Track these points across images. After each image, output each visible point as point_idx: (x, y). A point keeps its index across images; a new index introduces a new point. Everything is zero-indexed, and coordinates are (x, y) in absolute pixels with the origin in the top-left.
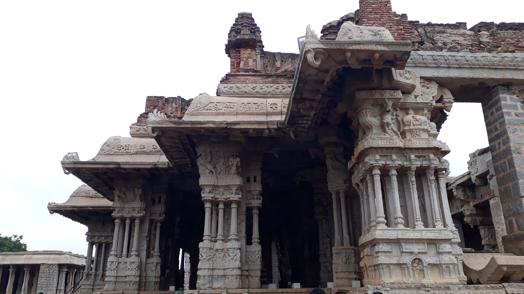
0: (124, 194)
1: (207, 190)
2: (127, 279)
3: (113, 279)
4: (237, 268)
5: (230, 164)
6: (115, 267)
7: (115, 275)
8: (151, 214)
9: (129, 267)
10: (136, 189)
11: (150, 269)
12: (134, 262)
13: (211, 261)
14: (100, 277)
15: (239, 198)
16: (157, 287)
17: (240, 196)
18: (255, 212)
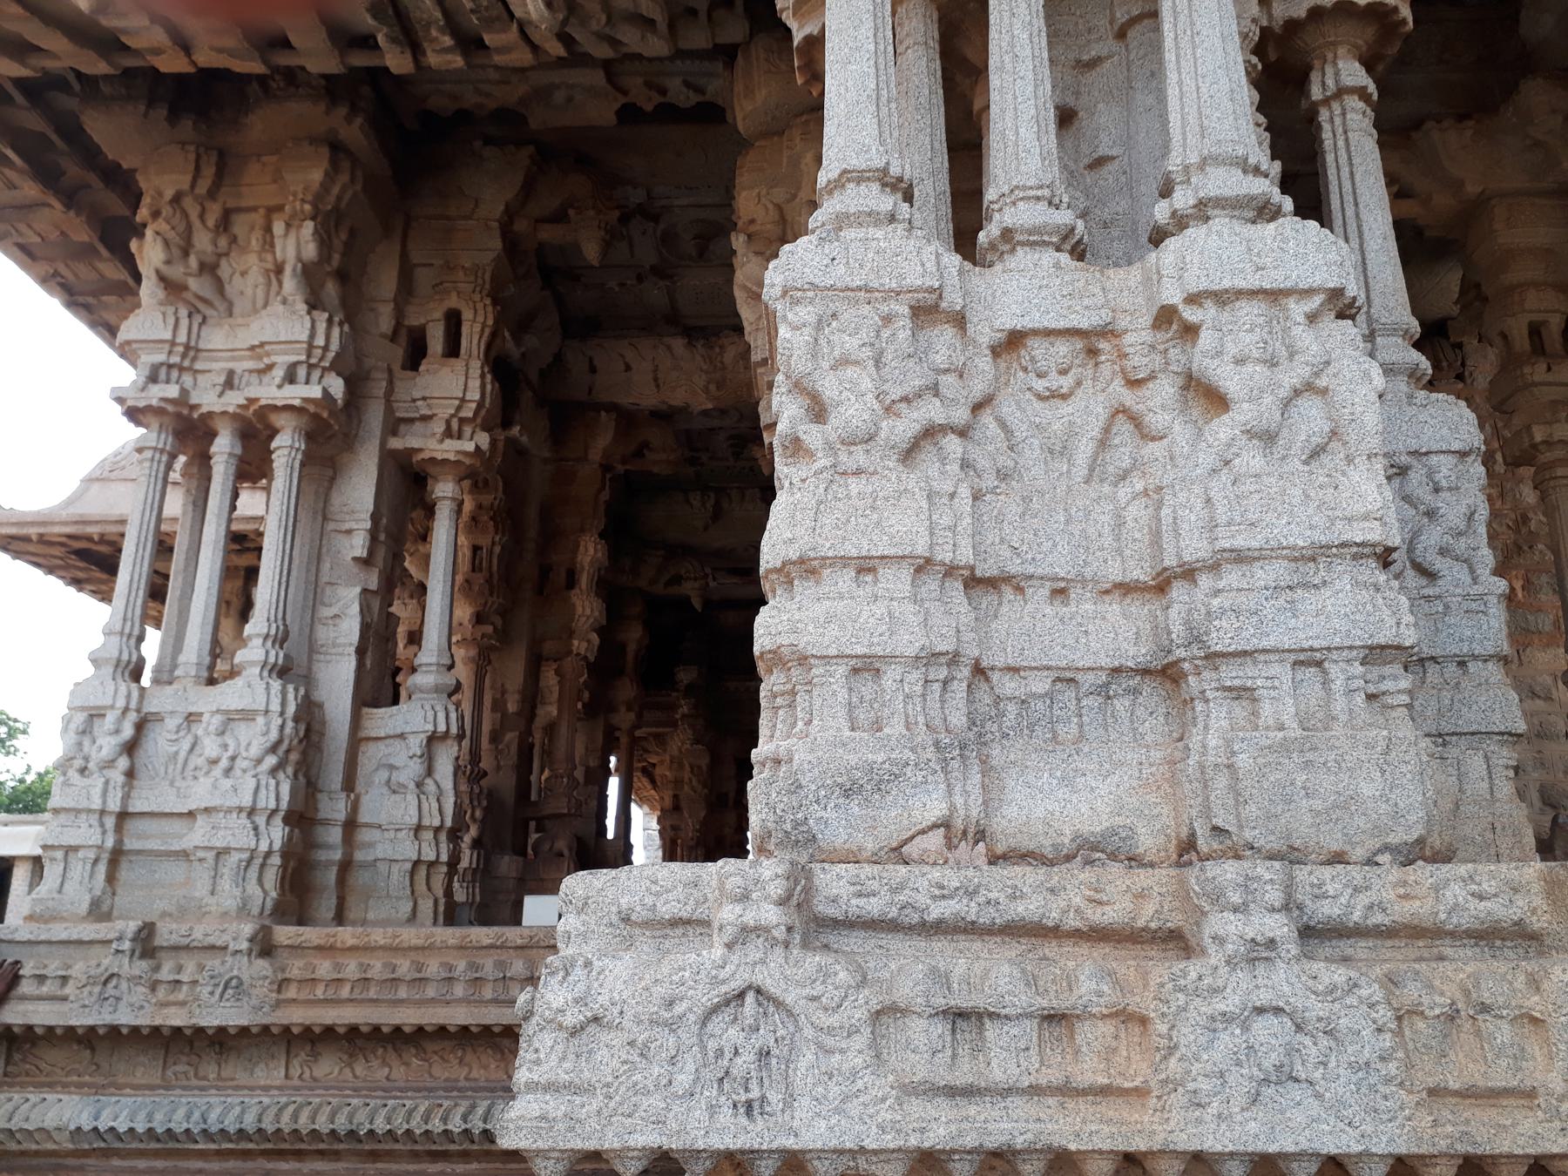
0: (209, 269)
8: (394, 425)
9: (210, 747)
11: (384, 774)
12: (247, 715)
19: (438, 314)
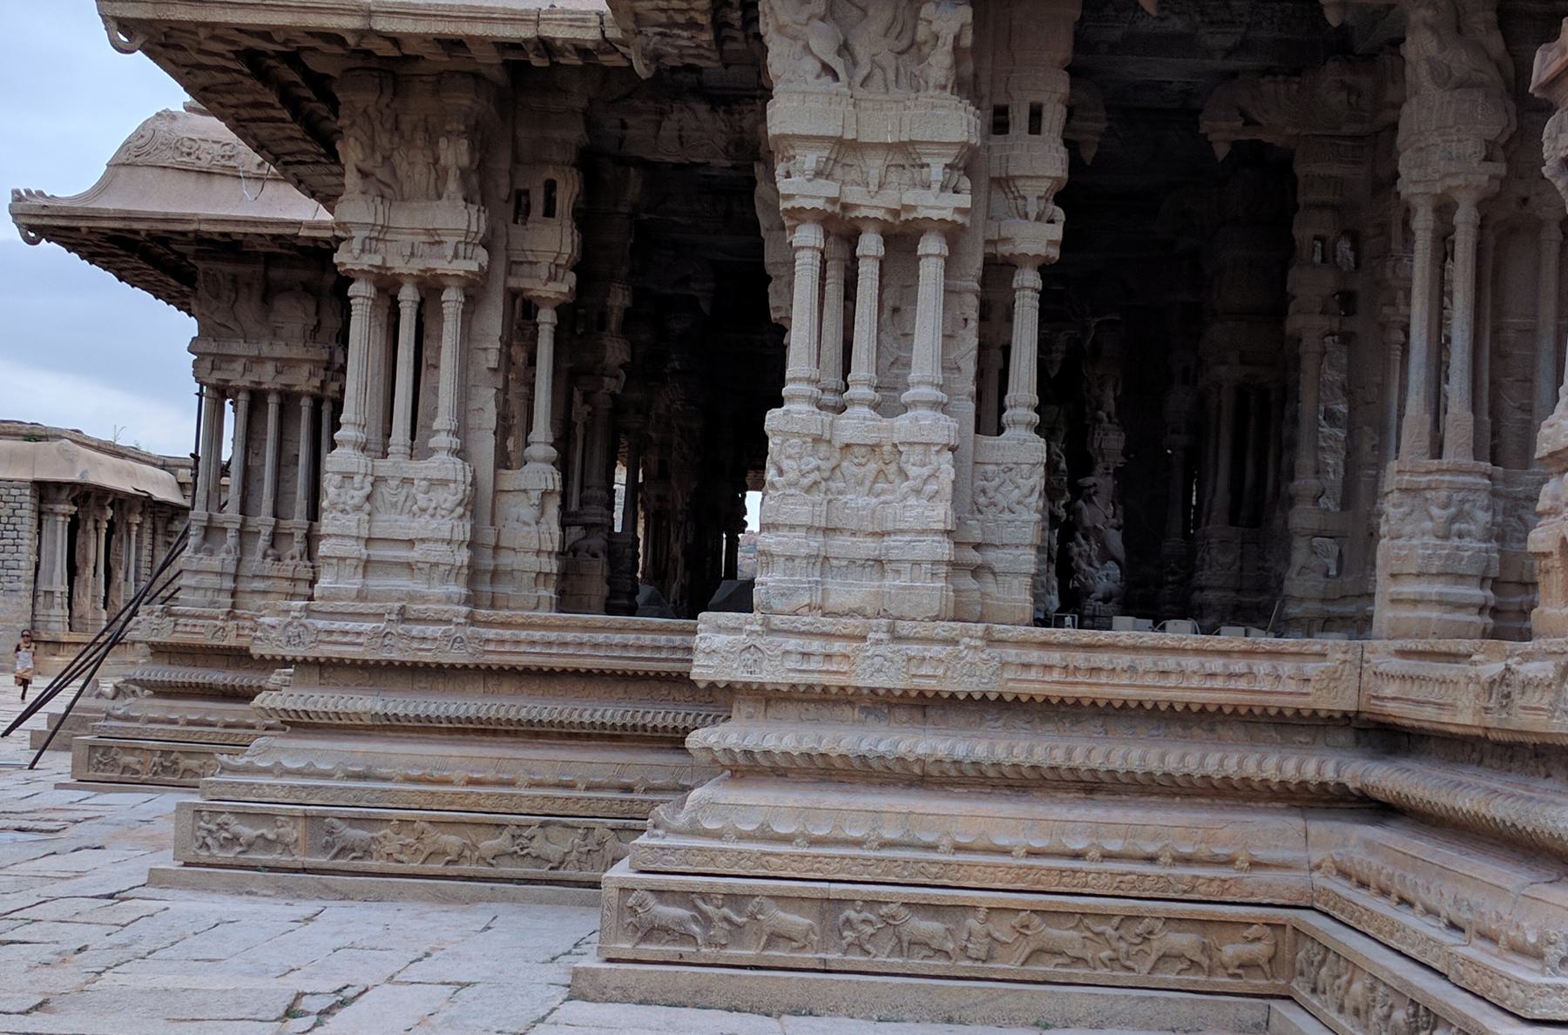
1: (810, 159)
2: (415, 554)
3: (356, 549)
4: (936, 532)
5: (922, 32)
6: (359, 496)
7: (365, 534)
8: (512, 267)
9: (422, 500)
10: (443, 143)
12: (444, 483)
13: (818, 497)
14: (262, 542)
15: (958, 210)
16: (548, 593)
17: (965, 200)
18: (1028, 280)
19: (540, 183)
